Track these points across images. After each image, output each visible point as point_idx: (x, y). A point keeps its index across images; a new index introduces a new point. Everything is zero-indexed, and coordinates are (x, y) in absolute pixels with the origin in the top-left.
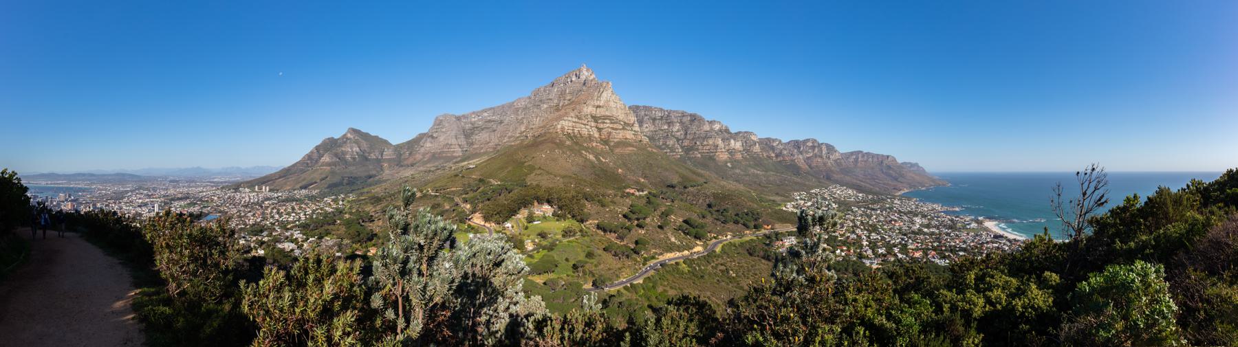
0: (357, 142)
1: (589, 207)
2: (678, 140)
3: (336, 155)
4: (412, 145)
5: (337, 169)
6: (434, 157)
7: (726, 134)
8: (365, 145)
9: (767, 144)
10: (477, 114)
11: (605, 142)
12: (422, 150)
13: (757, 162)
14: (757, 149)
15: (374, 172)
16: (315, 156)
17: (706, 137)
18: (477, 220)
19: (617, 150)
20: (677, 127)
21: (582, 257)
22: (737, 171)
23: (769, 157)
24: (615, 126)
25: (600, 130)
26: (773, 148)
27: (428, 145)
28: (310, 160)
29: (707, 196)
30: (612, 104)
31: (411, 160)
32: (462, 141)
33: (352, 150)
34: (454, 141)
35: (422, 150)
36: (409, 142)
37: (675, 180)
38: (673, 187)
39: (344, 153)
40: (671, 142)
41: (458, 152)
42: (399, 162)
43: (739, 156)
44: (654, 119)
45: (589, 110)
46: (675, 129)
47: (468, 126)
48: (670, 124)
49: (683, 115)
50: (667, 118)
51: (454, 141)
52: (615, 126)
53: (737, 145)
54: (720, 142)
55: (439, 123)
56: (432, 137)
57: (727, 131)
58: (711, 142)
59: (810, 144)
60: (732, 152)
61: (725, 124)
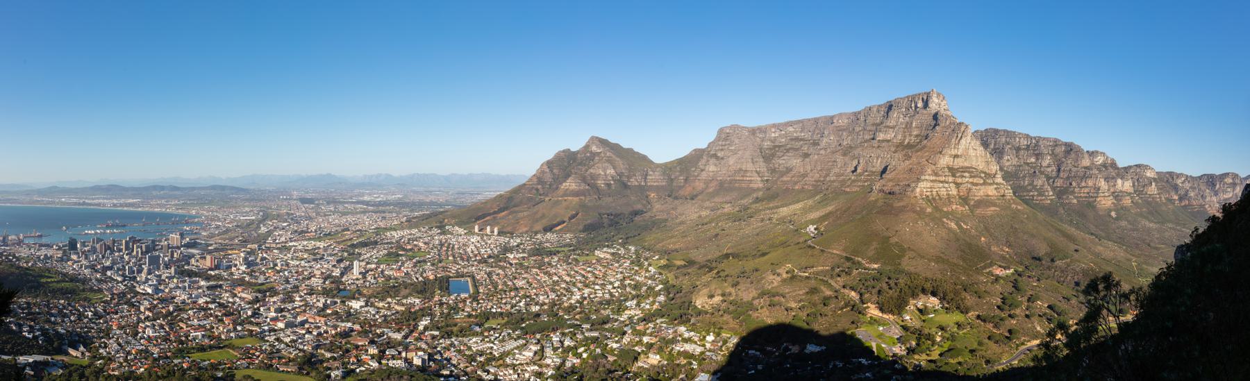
0: (610, 161)
1: (969, 299)
2: (1048, 178)
3: (584, 180)
4: (689, 164)
6: (724, 187)
7: (1111, 170)
8: (620, 164)
9: (1168, 180)
10: (777, 126)
11: (964, 200)
12: (704, 175)
13: (1152, 209)
14: (1153, 189)
15: (639, 207)
16: (548, 177)
17: (1085, 177)
18: (873, 311)
19: (978, 211)
20: (1047, 160)
21: (975, 346)
22: (1124, 223)
23: (1170, 201)
25: (958, 185)
26: (1176, 188)
27: (712, 168)
29: (1076, 273)
30: (972, 152)
31: (687, 191)
32: (762, 166)
33: (605, 172)
34: (750, 167)
35: (704, 175)
36: (680, 162)
37: (1042, 249)
38: (1039, 259)
40: (1039, 182)
41: (758, 183)
43: (1127, 201)
44: (1018, 149)
46: (1045, 163)
47: (767, 144)
48: (1038, 156)
49: (1056, 143)
50: (1035, 147)
53: (1125, 185)
54: (1103, 184)
55: (725, 136)
56: (715, 156)
57: (1114, 165)
58: (1090, 183)
59: (1229, 180)
60: (1117, 196)
61: (1111, 155)
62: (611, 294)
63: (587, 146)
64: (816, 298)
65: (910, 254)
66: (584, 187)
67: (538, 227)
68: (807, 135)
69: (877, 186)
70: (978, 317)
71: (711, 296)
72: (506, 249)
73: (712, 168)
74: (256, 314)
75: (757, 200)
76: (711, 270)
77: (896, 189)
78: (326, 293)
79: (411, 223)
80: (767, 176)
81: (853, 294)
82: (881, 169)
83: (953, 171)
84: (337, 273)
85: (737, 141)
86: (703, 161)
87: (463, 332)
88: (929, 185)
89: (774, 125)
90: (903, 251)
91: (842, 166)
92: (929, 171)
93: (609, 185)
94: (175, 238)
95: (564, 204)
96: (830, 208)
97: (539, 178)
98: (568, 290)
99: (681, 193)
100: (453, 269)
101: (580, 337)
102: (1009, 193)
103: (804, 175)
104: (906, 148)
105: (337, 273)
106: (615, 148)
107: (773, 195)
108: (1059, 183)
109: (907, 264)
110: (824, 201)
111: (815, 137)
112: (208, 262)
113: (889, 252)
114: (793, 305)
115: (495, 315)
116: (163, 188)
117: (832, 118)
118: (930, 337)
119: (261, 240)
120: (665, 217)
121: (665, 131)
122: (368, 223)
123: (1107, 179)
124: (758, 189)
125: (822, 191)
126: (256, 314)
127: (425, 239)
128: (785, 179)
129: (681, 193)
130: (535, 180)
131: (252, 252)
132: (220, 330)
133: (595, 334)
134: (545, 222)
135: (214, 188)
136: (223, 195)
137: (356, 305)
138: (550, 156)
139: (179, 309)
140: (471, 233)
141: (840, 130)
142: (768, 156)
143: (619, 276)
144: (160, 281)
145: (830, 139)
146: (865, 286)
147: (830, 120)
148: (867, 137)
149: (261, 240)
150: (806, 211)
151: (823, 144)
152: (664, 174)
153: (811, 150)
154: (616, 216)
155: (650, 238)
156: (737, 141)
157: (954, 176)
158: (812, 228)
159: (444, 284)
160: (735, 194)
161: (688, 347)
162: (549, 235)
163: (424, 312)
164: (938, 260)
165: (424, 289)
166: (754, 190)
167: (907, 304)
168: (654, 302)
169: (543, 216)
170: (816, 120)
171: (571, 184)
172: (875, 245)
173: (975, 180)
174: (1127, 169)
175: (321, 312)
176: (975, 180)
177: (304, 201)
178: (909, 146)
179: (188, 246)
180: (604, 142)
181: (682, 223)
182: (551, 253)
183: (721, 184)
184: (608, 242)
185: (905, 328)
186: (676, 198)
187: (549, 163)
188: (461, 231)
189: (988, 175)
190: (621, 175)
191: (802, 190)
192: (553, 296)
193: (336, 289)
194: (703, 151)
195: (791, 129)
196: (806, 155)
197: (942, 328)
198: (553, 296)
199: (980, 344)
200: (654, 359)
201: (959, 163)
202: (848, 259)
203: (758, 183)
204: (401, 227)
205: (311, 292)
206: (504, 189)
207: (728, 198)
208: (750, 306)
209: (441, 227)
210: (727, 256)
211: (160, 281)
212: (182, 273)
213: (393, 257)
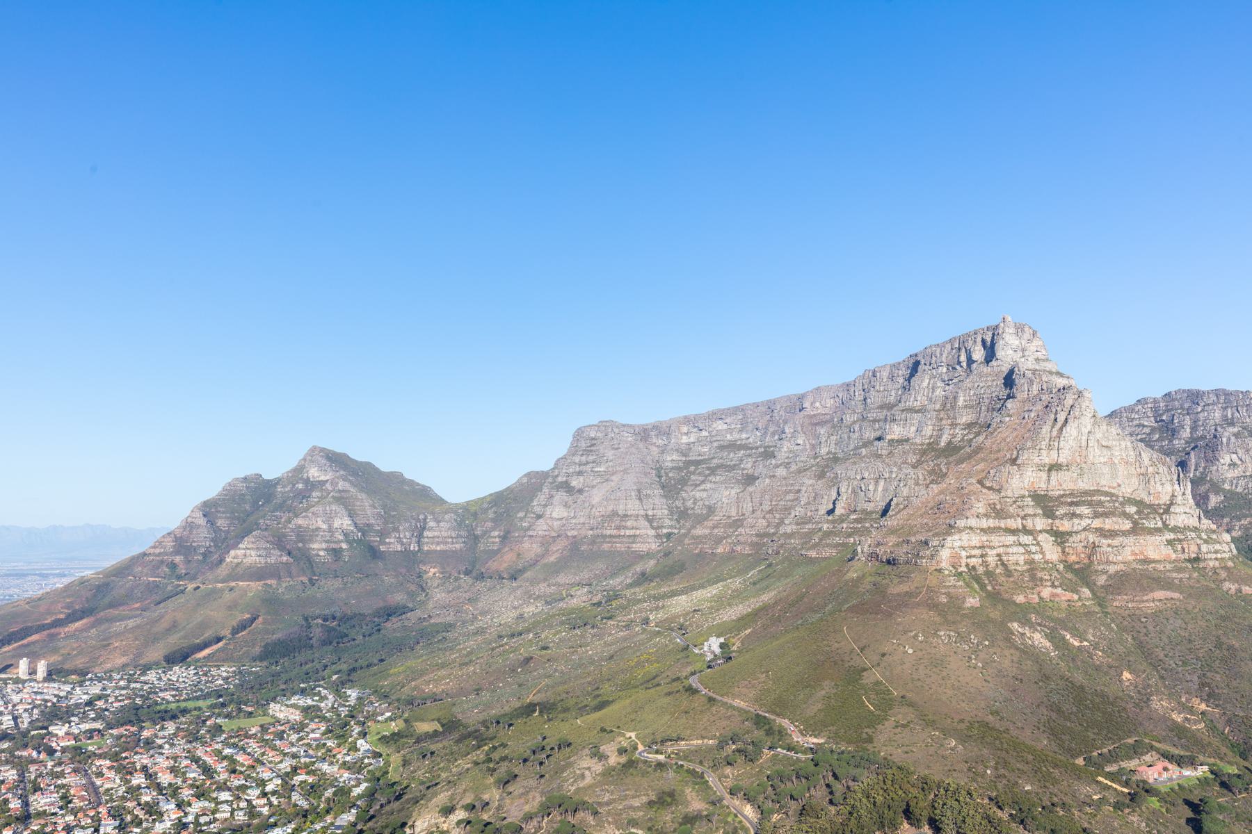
0: (342, 499)
3: (280, 542)
4: (508, 505)
5: (282, 587)
6: (578, 552)
8: (368, 509)
12: (541, 527)
15: (399, 598)
16: (202, 538)
24: (1108, 524)
28: (189, 555)
31: (506, 560)
32: (658, 506)
33: (328, 525)
34: (633, 507)
35: (541, 527)
36: (498, 499)
39: (304, 535)
41: (648, 542)
42: (472, 565)
51: (633, 507)
52: (1108, 524)
56: (566, 487)
63: (299, 469)
67: (156, 653)
68: (753, 438)
69: (864, 548)
72: (56, 713)
73: (558, 512)
75: (644, 578)
77: (901, 553)
80: (668, 525)
82: (882, 504)
83: (1046, 503)
85: (610, 454)
86: (541, 498)
88: (976, 540)
91: (813, 500)
92: (980, 507)
93: (336, 553)
95: (227, 596)
97: (182, 543)
99: (493, 565)
103: (738, 523)
104: (940, 456)
106: (363, 474)
107: (675, 568)
110: (758, 585)
111: (768, 441)
117: (801, 398)
121: (465, 439)
124: (649, 555)
125: (765, 557)
128: (699, 531)
130: (169, 544)
134: (175, 641)
138: (212, 489)
141: (817, 422)
142: (673, 483)
147: (798, 403)
148: (869, 435)
151: (782, 455)
152: (460, 524)
153: (760, 469)
154: (345, 619)
156: (610, 454)
157: (1049, 514)
160: (600, 566)
166: (640, 557)
169: (174, 626)
170: (770, 406)
171: (247, 553)
180: (336, 460)
183: (575, 544)
184: (306, 681)
186: (481, 577)
187: (209, 509)
190: (365, 529)
191: (731, 556)
194: (543, 476)
195: (720, 425)
196: (750, 479)
201: (1062, 483)
203: (648, 542)
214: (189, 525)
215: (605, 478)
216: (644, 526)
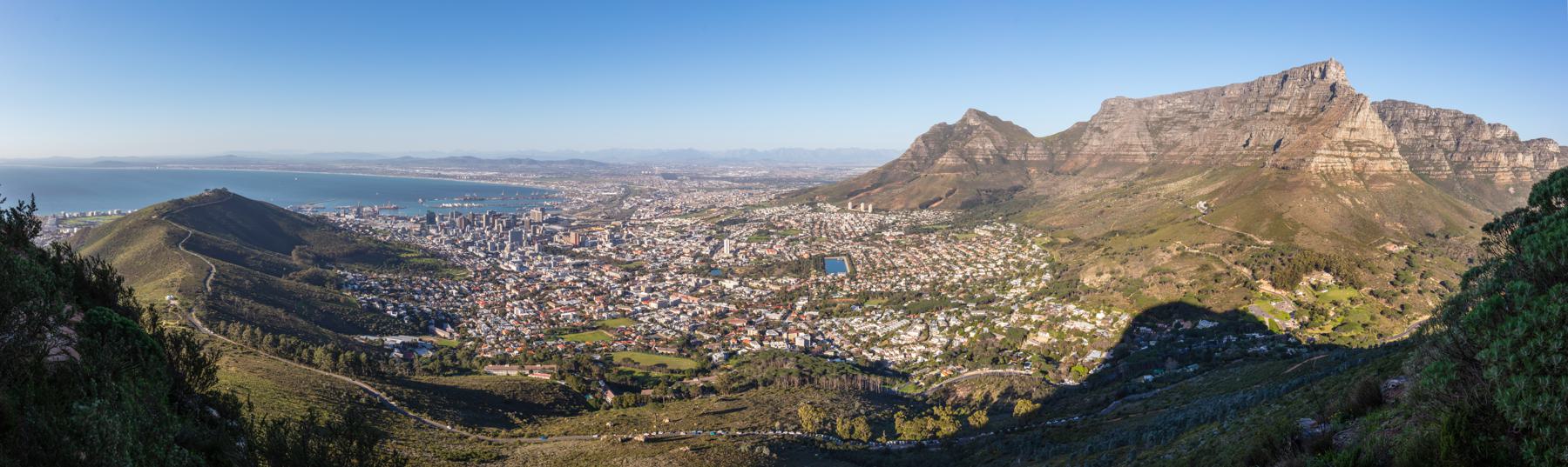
0: (988, 134)
1: (1363, 275)
2: (1446, 152)
3: (961, 155)
4: (1070, 138)
5: (964, 176)
6: (1107, 162)
7: (1513, 144)
8: (999, 137)
11: (1360, 175)
12: (1087, 150)
15: (1019, 183)
16: (924, 152)
17: (1485, 151)
18: (1266, 287)
19: (1373, 187)
20: (1446, 134)
21: (1368, 320)
25: (1353, 159)
31: (1070, 166)
32: (1148, 140)
33: (983, 147)
34: (1135, 140)
35: (1087, 150)
36: (1062, 135)
37: (1437, 226)
39: (972, 152)
40: (1436, 157)
41: (1144, 158)
42: (1052, 168)
44: (1417, 122)
45: (1341, 134)
47: (1154, 117)
48: (1437, 129)
49: (1457, 115)
50: (1434, 119)
54: (1503, 159)
55: (1109, 109)
56: (1099, 129)
57: (1515, 138)
58: (1490, 157)
60: (1517, 171)
61: (1513, 128)
62: (994, 273)
63: (964, 120)
64: (1207, 275)
65: (1303, 230)
66: (961, 162)
67: (914, 204)
68: (1195, 107)
69: (1270, 161)
70: (1371, 293)
71: (1100, 274)
72: (882, 227)
73: (1095, 142)
74: (626, 293)
75: (1143, 176)
76: (1098, 247)
77: (1290, 164)
78: (697, 272)
79: (780, 200)
80: (1153, 150)
81: (1245, 270)
82: (1274, 142)
83: (1349, 145)
84: (706, 251)
86: (1086, 135)
87: (843, 312)
89: (1162, 97)
90: (1297, 227)
91: (1234, 140)
93: (987, 160)
94: (536, 214)
96: (1220, 184)
97: (914, 153)
98: (949, 269)
99: (1063, 168)
100: (828, 248)
101: (966, 316)
102: (1406, 167)
103: (1193, 150)
105: (706, 251)
106: (994, 121)
107: (1159, 170)
108: (1457, 157)
109: (1301, 240)
110: (1213, 177)
112: (572, 239)
113: (1283, 228)
114: (1184, 282)
115: (874, 295)
116: (519, 161)
117: (1223, 89)
118: (1323, 312)
119: (625, 217)
120: (1046, 193)
122: (735, 199)
123: (1507, 154)
124: (1144, 164)
125: (1211, 166)
126: (626, 293)
127: (796, 216)
129: (1063, 168)
131: (616, 229)
132: (590, 310)
133: (982, 313)
134: (921, 199)
135: (572, 162)
136: (582, 169)
137: (729, 284)
138: (925, 130)
139: (545, 288)
140: (844, 210)
141: (1231, 101)
142: (1155, 129)
143: (1002, 254)
144: (524, 259)
145: (1220, 112)
146: (1258, 262)
148: (1260, 109)
149: (625, 217)
150: (1194, 187)
151: (1213, 117)
152: (1045, 148)
153: (1200, 123)
154: (996, 191)
155: (1031, 215)
158: (1201, 204)
159: (820, 263)
160: (1119, 170)
161: (1079, 325)
162: (925, 212)
163: (801, 292)
164: (1332, 236)
165: (798, 268)
166: (1140, 165)
167: (1300, 279)
168: (1039, 281)
169: (919, 193)
170: (1206, 92)
171: (947, 159)
172: (1268, 221)
173: (1372, 155)
174: (1529, 143)
175: (694, 291)
176: (1372, 155)
177: (666, 176)
178: (1305, 119)
179: (550, 221)
180: (981, 115)
181: (1064, 199)
182: (929, 231)
183: (1105, 158)
184: (988, 219)
185: (1298, 303)
186: (1058, 174)
187: (925, 138)
188: (833, 208)
189: (1385, 149)
190: (999, 149)
191: (1190, 165)
192: (934, 275)
193: (707, 268)
194: (1086, 124)
195: (1179, 101)
196: (1195, 129)
197: (1336, 304)
198: (934, 275)
199: (1373, 318)
200: (1043, 337)
201: (1356, 136)
202: (1240, 236)
203: (1144, 158)
204: (770, 204)
205: (682, 271)
206: (877, 164)
207: (1112, 174)
208: (1141, 283)
209: (812, 204)
210: (1114, 233)
211: (524, 259)
212: (546, 250)
213: (763, 235)
214: (918, 147)
215: (1119, 126)
216: (1141, 150)
